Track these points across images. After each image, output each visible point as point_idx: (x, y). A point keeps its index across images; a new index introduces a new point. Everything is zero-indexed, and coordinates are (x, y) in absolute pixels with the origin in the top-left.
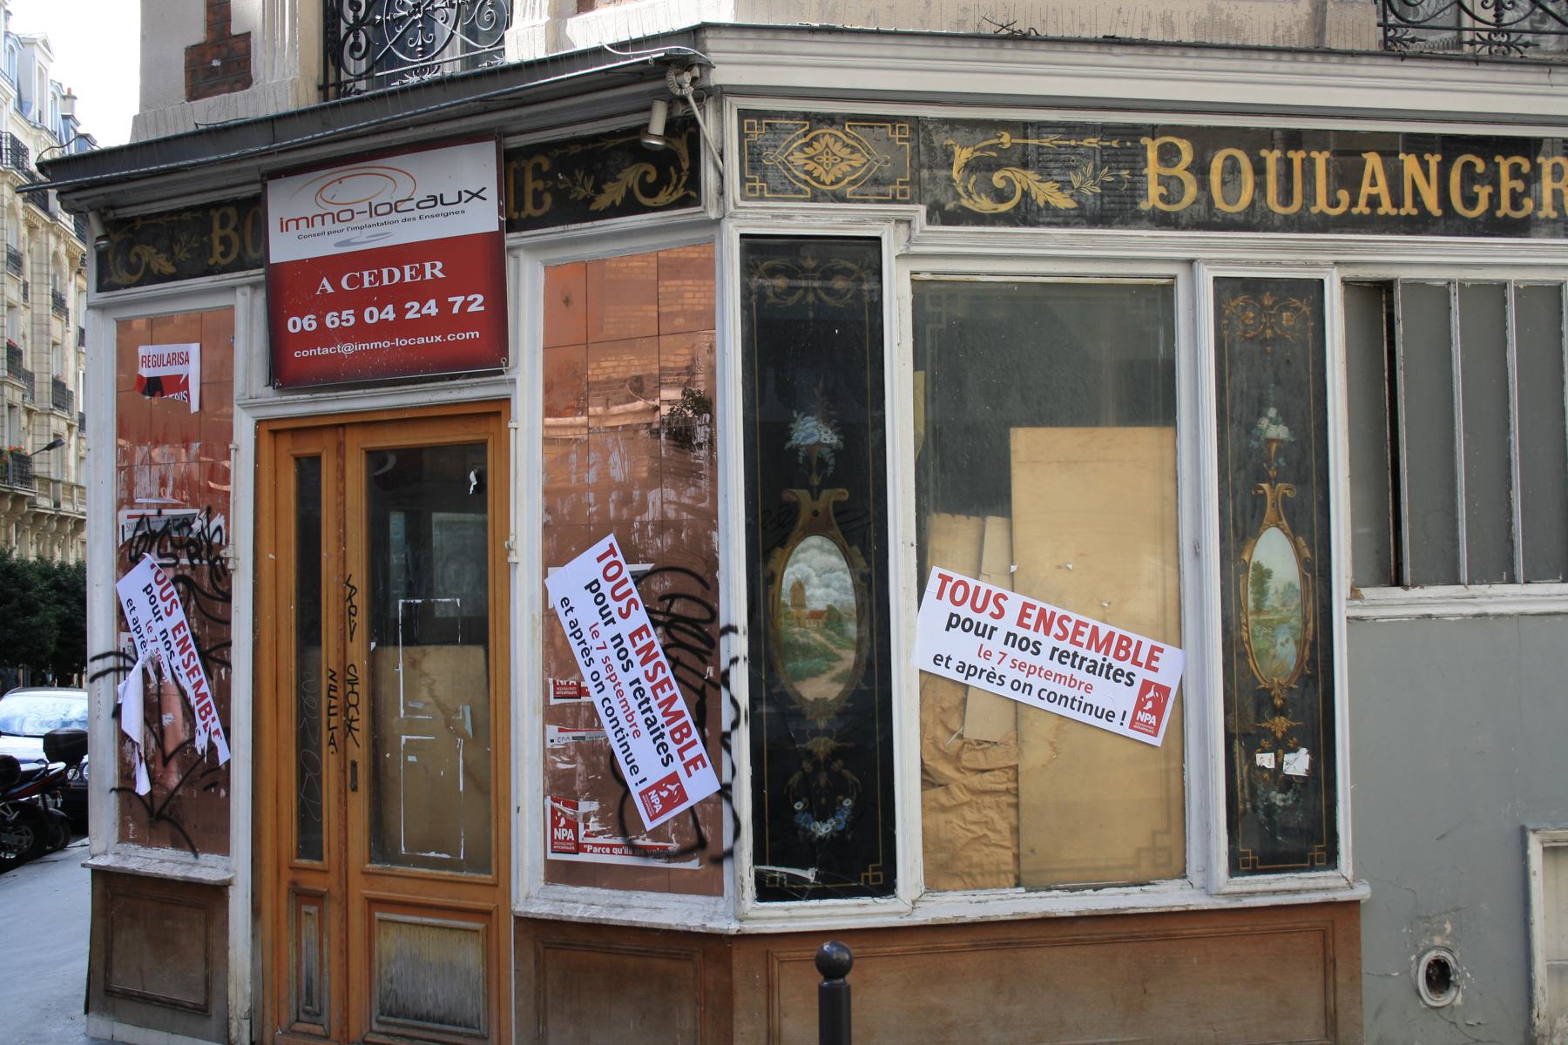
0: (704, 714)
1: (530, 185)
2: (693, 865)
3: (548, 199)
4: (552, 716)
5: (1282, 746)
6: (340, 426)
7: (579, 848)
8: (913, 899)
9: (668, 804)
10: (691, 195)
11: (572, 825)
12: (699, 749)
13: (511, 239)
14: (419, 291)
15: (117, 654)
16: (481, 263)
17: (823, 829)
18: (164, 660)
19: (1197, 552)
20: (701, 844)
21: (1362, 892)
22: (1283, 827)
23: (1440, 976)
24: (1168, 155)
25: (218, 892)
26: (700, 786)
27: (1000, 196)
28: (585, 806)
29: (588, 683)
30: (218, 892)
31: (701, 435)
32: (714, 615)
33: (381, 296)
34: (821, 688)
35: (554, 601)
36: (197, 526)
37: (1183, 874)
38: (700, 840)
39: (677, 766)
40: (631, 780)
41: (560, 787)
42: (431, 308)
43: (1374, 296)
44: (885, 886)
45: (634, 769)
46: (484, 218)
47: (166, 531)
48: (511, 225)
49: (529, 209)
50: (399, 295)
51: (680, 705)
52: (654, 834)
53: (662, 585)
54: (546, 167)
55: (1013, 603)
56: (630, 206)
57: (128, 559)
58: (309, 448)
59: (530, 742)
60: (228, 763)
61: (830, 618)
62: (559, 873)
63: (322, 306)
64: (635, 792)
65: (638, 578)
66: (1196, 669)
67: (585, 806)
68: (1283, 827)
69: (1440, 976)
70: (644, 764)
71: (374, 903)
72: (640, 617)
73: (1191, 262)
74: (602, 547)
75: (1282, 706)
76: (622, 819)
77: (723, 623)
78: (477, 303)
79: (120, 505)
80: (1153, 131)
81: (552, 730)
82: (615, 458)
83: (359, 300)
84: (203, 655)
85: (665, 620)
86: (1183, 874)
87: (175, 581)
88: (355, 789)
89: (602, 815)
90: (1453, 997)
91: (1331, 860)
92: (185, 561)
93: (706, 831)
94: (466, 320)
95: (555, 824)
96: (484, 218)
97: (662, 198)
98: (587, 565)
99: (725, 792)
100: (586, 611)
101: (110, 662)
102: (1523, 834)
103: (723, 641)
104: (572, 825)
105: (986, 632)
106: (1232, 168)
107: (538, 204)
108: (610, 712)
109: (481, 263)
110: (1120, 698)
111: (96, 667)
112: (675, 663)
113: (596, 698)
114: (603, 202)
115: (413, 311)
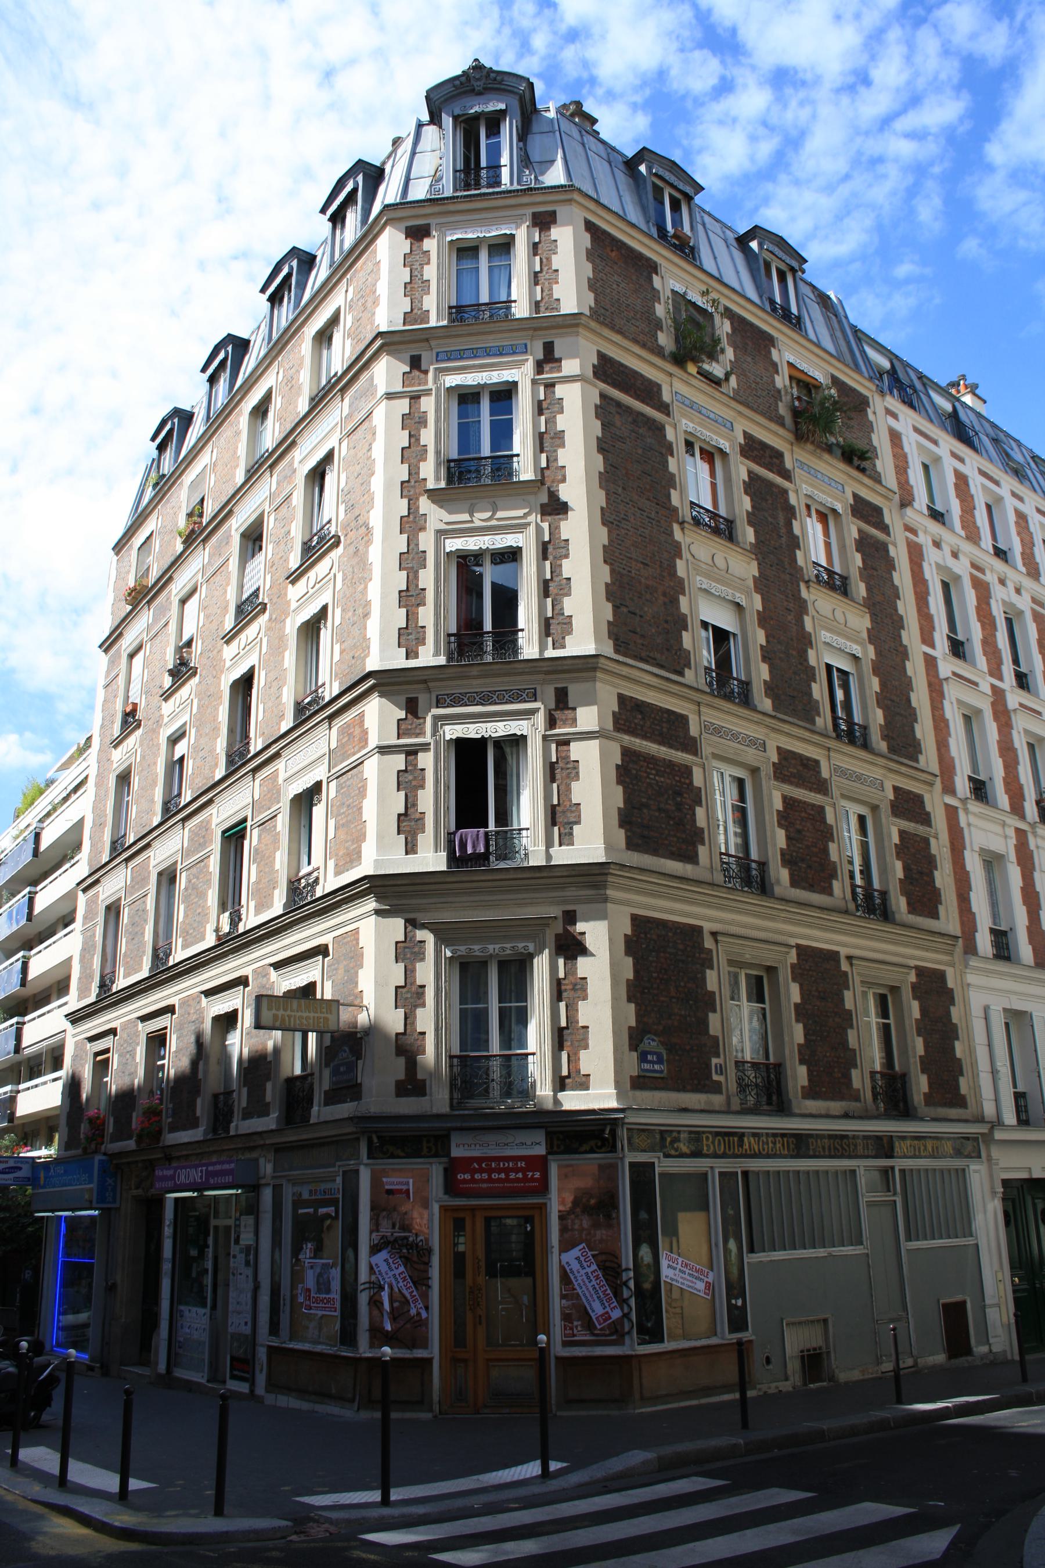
0: (617, 1294)
1: (555, 1142)
2: (614, 1337)
3: (562, 1148)
4: (563, 1297)
5: (736, 1298)
6: (473, 1209)
7: (574, 1335)
8: (668, 1346)
9: (605, 1320)
10: (613, 1149)
11: (571, 1329)
12: (615, 1304)
13: (550, 1157)
14: (517, 1170)
15: (370, 1283)
16: (541, 1164)
17: (649, 1325)
18: (394, 1284)
19: (717, 1245)
20: (616, 1331)
21: (753, 1338)
22: (738, 1320)
23: (768, 1361)
24: (707, 1138)
25: (429, 1361)
26: (616, 1314)
27: (676, 1150)
28: (575, 1323)
29: (576, 1286)
30: (429, 1361)
31: (614, 1215)
32: (620, 1266)
33: (499, 1171)
34: (647, 1286)
35: (564, 1263)
36: (411, 1239)
37: (716, 1335)
38: (616, 1332)
39: (608, 1309)
40: (592, 1314)
41: (566, 1317)
42: (520, 1175)
43: (746, 1174)
44: (662, 1341)
45: (593, 1311)
46: (541, 1150)
47: (396, 1240)
48: (549, 1153)
49: (555, 1149)
50: (507, 1171)
51: (609, 1291)
52: (601, 1329)
53: (603, 1257)
54: (561, 1137)
55: (680, 1260)
56: (592, 1151)
57: (375, 1249)
58: (461, 1215)
59: (557, 1305)
60: (427, 1318)
61: (648, 1265)
62: (565, 1344)
63: (474, 1171)
64: (594, 1318)
65: (593, 1256)
66: (717, 1277)
67: (575, 1323)
68: (738, 1320)
69: (768, 1361)
70: (597, 1309)
71: (488, 1360)
72: (594, 1267)
73: (712, 1168)
74: (581, 1247)
75: (735, 1288)
76: (589, 1325)
77: (624, 1267)
78: (537, 1175)
79: (371, 1232)
80: (704, 1132)
81: (564, 1301)
82: (584, 1222)
83: (490, 1171)
84: (414, 1283)
85: (603, 1267)
86: (716, 1335)
87: (400, 1257)
88: (480, 1323)
89: (582, 1326)
90: (771, 1367)
91: (747, 1329)
92: (405, 1251)
93: (618, 1327)
94: (533, 1180)
95: (565, 1329)
96: (541, 1150)
97: (603, 1150)
98: (576, 1252)
99: (626, 1315)
100: (575, 1266)
101: (367, 1286)
102: (782, 1320)
103: (624, 1274)
104: (571, 1329)
105: (675, 1269)
106: (719, 1141)
107: (558, 1146)
108: (584, 1295)
109: (541, 1164)
110: (701, 1286)
111: (363, 1287)
112: (607, 1280)
113: (580, 1291)
114: (583, 1149)
115: (512, 1176)
